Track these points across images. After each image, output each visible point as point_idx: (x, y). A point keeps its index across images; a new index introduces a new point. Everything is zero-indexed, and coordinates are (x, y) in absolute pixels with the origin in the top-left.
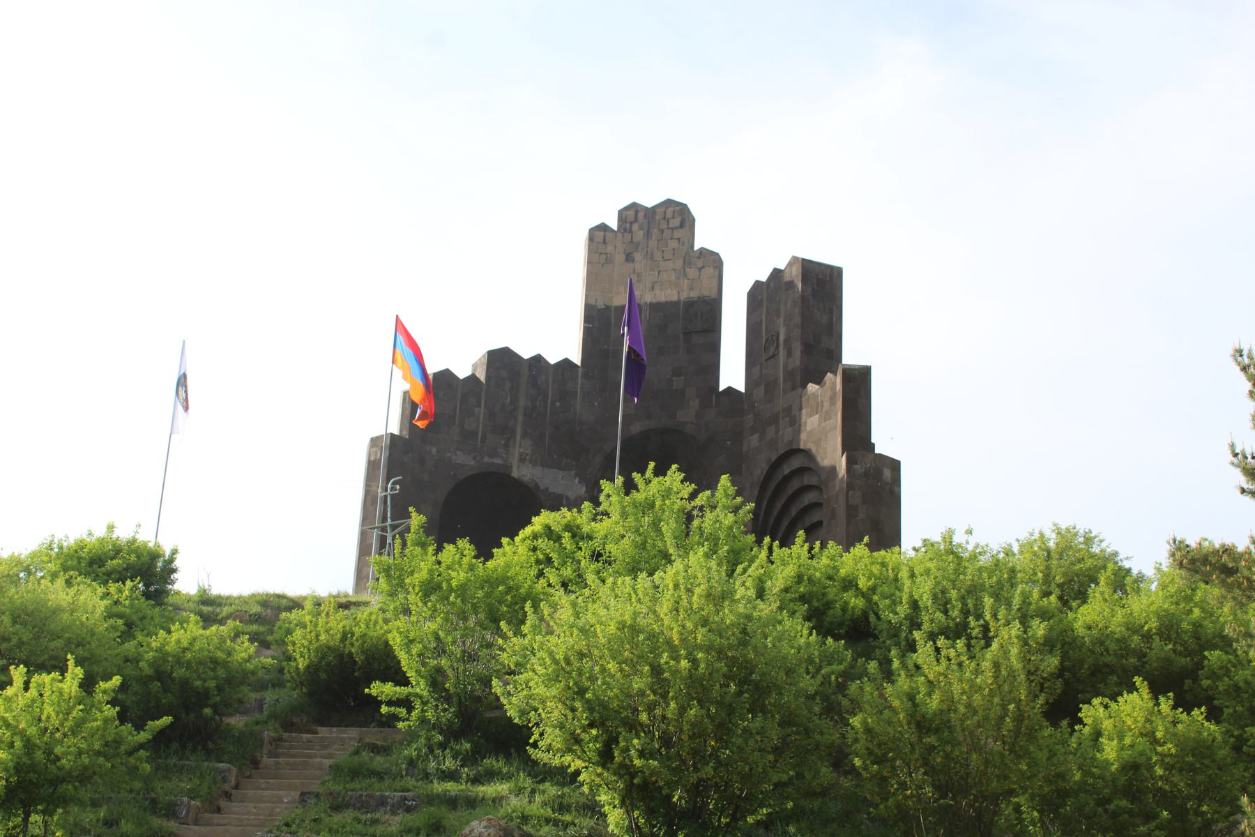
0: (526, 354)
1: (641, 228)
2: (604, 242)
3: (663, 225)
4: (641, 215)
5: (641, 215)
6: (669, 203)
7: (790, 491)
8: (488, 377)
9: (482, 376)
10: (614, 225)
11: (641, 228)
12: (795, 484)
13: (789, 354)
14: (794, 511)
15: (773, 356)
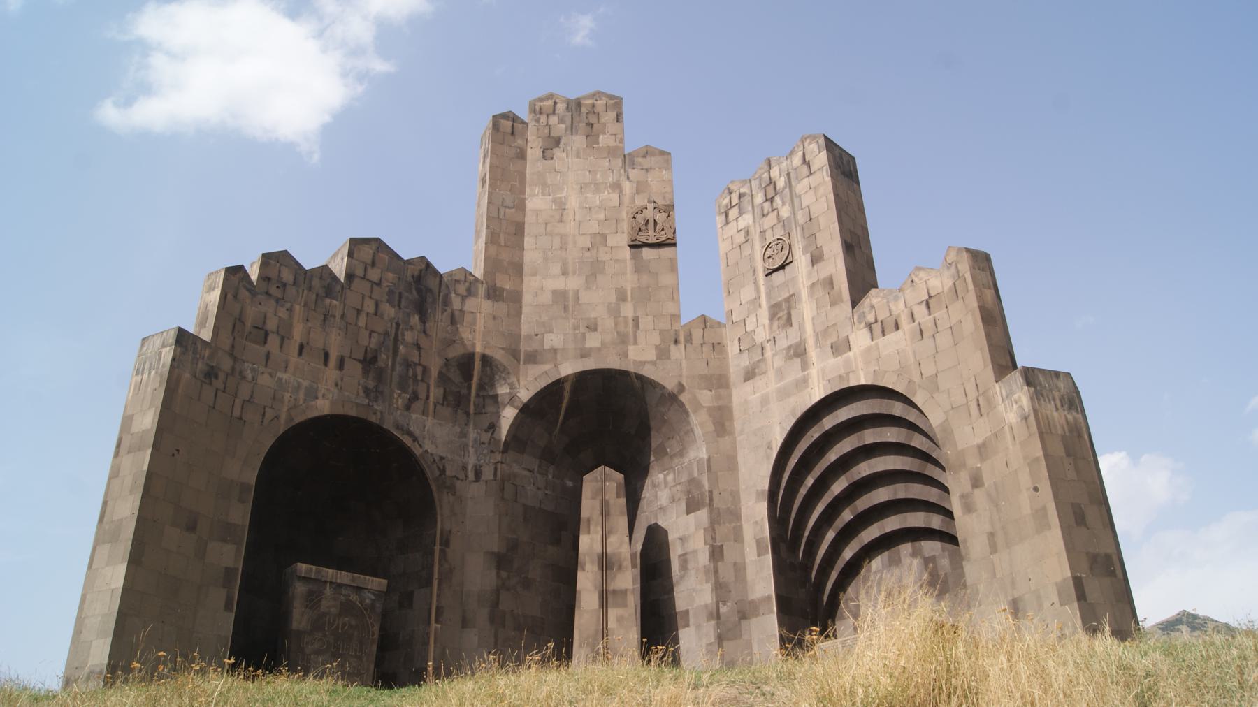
0: (407, 252)
1: (561, 121)
2: (512, 133)
3: (592, 119)
4: (561, 107)
5: (561, 107)
6: (598, 95)
7: (833, 456)
8: (350, 276)
9: (339, 268)
10: (524, 114)
11: (561, 121)
12: (846, 446)
13: (816, 259)
14: (838, 487)
15: (782, 267)
